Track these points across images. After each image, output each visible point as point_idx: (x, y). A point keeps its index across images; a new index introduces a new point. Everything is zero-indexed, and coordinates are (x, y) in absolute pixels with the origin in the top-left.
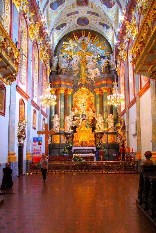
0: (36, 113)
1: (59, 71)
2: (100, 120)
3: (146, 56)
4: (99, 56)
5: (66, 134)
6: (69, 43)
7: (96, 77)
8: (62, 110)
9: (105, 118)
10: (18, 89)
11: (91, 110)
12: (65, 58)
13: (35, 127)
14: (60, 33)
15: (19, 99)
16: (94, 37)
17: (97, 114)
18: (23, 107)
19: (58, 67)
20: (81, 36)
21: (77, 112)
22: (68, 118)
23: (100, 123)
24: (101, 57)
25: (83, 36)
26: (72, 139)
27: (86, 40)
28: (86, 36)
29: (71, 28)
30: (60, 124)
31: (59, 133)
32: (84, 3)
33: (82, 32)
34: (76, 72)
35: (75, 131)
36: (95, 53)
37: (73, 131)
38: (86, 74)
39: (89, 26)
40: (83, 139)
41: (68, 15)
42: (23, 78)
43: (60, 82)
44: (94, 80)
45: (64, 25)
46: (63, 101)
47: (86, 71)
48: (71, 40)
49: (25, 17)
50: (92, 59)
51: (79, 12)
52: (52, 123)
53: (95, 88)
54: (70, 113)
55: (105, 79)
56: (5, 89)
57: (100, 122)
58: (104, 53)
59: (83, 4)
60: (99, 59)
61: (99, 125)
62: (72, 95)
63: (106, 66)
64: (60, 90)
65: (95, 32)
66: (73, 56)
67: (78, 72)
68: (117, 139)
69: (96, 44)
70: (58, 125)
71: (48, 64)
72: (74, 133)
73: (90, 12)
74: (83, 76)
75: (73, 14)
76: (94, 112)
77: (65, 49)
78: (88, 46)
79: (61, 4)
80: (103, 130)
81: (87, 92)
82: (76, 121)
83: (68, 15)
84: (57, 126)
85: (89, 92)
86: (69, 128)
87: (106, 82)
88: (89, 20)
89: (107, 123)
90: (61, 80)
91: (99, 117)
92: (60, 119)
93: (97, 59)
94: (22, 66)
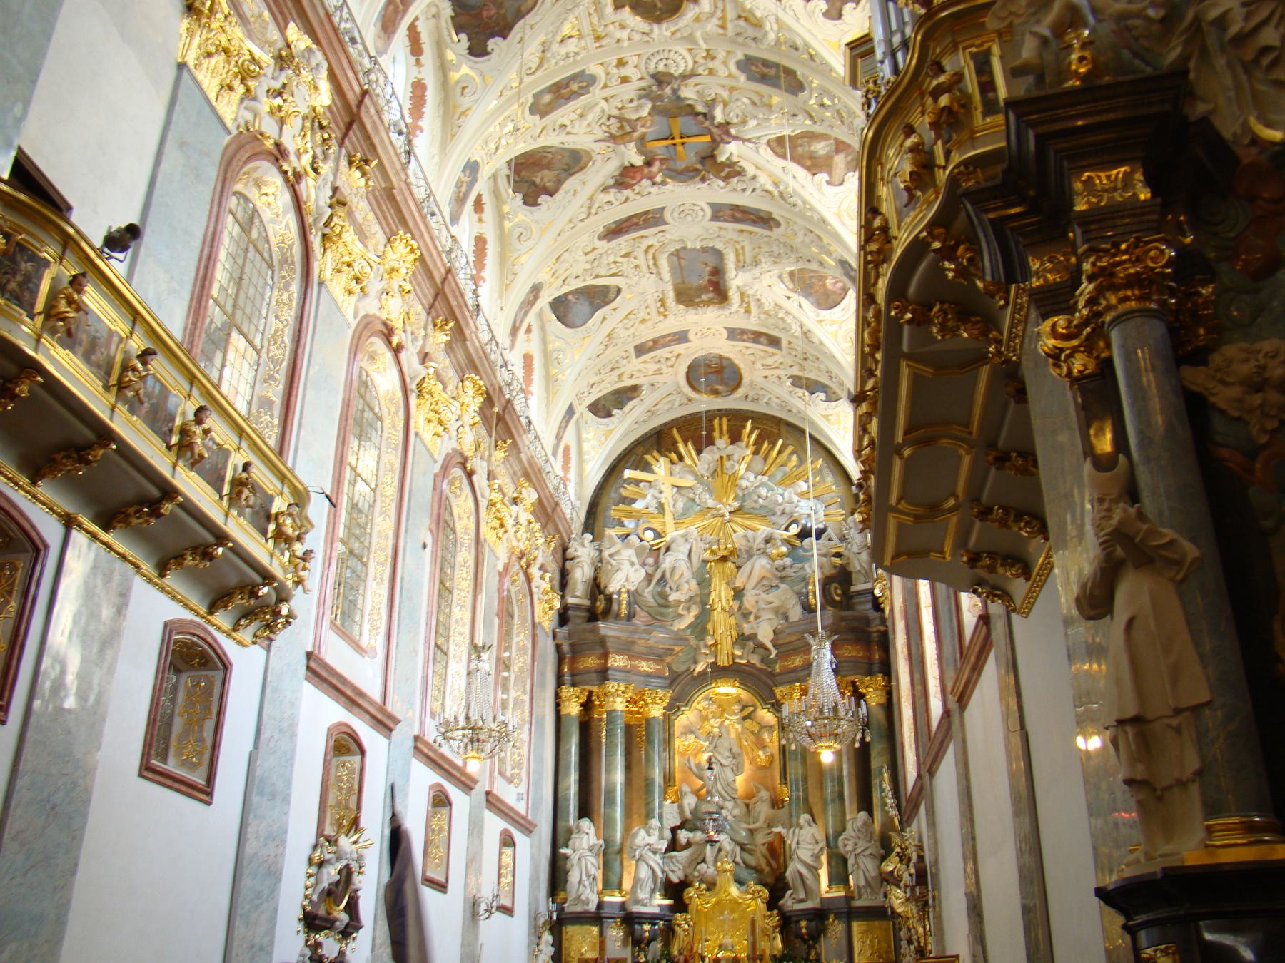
0: (451, 805)
1: (601, 605)
2: (805, 842)
3: (897, 464)
4: (794, 530)
5: (630, 920)
6: (653, 472)
7: (783, 632)
10: (319, 673)
11: (764, 794)
12: (628, 546)
13: (443, 880)
14: (611, 431)
15: (328, 725)
16: (774, 444)
17: (791, 816)
18: (357, 766)
19: (596, 587)
20: (711, 442)
21: (693, 807)
23: (809, 860)
24: (804, 534)
25: (722, 442)
27: (736, 457)
28: (735, 438)
29: (663, 406)
30: (606, 866)
31: (597, 918)
32: (711, 295)
33: (716, 422)
34: (688, 609)
35: (680, 906)
36: (775, 514)
37: (667, 902)
38: (738, 615)
39: (747, 397)
41: (640, 350)
42: (366, 627)
43: (605, 656)
44: (770, 646)
45: (629, 394)
47: (736, 605)
48: (662, 460)
49: (390, 343)
50: (762, 546)
51: (691, 336)
52: (560, 863)
54: (654, 810)
56: (226, 667)
57: (805, 854)
58: (821, 513)
59: (705, 297)
60: (797, 543)
61: (804, 871)
62: (668, 722)
63: (830, 571)
65: (778, 421)
66: (671, 533)
67: (695, 611)
68: (897, 939)
69: (779, 476)
71: (542, 568)
73: (743, 332)
74: (723, 629)
75: (664, 346)
76: (776, 803)
77: (634, 501)
78: (744, 483)
79: (606, 304)
81: (744, 707)
83: (640, 350)
84: (588, 876)
86: (648, 889)
88: (742, 366)
89: (845, 861)
90: (611, 649)
92: (605, 841)
93: (787, 542)
94: (365, 565)
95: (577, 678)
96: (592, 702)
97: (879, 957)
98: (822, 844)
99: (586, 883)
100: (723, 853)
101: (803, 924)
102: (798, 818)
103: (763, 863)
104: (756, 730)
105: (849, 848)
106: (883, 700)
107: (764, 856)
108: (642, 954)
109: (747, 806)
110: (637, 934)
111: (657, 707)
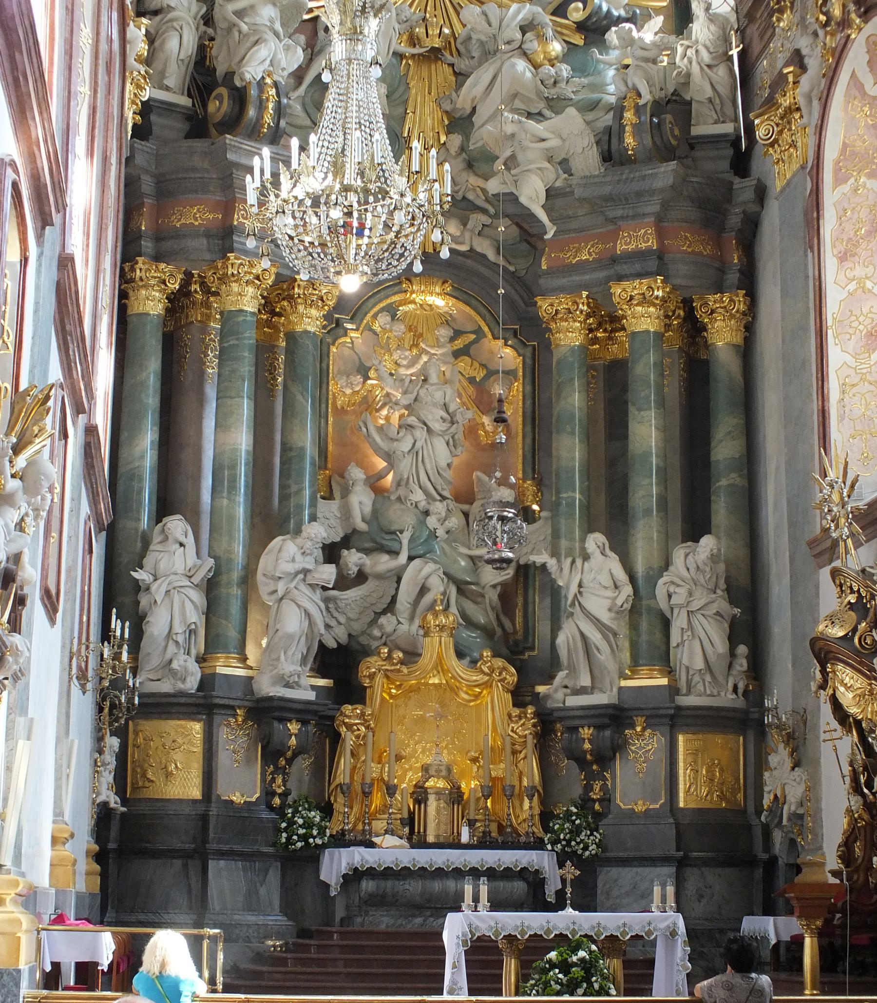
5: (264, 713)
8: (233, 481)
9: (640, 569)
21: (368, 509)
22: (289, 555)
23: (605, 617)
26: (324, 768)
37: (322, 682)
40: (425, 769)
47: (456, 140)
50: (519, 36)
53: (544, 294)
54: (300, 508)
55: (655, 208)
61: (595, 636)
64: (224, 279)
70: (195, 617)
72: (347, 709)
80: (624, 683)
81: (457, 334)
82: (352, 594)
85: (478, 332)
87: (661, 235)
89: (666, 624)
91: (586, 557)
92: (217, 559)
95: (168, 245)
96: (188, 294)
97: (722, 797)
98: (628, 590)
99: (180, 639)
101: (586, 732)
102: (583, 540)
103: (492, 616)
104: (480, 375)
106: (738, 339)
107: (492, 608)
108: (279, 781)
109: (466, 515)
111: (314, 312)
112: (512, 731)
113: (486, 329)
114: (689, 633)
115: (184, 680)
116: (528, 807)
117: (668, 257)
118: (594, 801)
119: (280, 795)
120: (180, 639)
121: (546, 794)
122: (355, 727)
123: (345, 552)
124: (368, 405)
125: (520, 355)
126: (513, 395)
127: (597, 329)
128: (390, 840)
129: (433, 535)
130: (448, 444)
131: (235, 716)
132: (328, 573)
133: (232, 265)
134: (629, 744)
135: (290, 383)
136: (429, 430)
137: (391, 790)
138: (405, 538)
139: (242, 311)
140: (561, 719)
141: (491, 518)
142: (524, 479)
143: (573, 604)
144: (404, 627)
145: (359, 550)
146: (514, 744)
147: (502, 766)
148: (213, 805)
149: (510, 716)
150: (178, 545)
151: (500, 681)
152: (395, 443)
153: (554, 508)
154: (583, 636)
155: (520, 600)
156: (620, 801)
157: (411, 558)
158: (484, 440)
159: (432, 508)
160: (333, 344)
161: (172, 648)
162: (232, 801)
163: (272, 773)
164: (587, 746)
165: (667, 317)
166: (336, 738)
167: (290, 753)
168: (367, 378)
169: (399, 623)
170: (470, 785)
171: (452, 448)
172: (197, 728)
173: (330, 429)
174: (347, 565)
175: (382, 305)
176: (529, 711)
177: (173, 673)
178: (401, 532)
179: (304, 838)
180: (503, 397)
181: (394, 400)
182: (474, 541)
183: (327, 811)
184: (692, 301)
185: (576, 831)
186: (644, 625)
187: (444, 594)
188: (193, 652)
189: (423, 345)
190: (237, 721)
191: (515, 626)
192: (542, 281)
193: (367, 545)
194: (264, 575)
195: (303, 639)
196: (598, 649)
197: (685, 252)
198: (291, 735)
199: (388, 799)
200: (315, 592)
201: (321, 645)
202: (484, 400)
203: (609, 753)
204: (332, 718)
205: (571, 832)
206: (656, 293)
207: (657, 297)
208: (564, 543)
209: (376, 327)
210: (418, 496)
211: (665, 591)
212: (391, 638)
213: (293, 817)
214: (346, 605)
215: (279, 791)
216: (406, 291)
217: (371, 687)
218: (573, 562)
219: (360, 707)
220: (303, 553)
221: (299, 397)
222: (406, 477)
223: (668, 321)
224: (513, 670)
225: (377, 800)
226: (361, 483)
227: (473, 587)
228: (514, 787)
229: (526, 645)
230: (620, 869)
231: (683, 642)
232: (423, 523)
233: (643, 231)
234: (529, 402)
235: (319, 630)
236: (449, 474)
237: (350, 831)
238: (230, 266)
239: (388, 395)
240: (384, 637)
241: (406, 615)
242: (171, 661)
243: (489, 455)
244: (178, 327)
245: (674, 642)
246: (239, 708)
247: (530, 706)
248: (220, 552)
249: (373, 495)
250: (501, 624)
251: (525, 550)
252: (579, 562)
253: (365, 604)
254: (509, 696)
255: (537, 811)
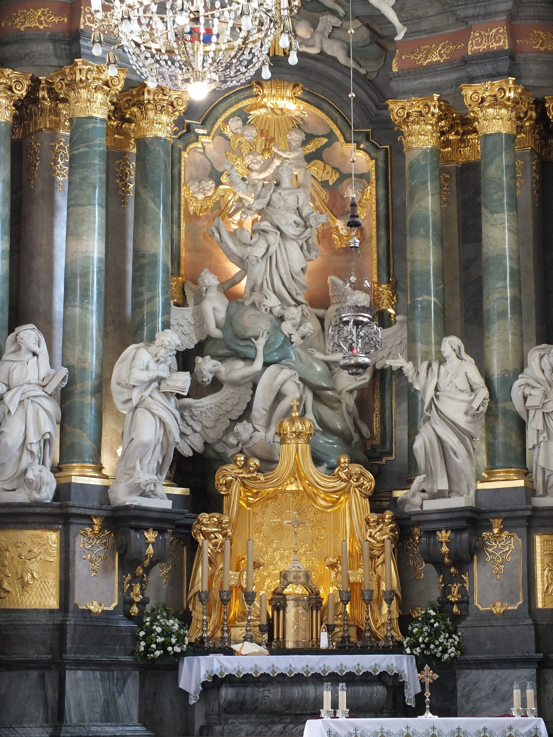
5: (121, 522)
8: (86, 289)
9: (496, 371)
21: (222, 315)
22: (144, 364)
23: (462, 420)
26: (182, 576)
30: (67, 418)
37: (178, 491)
40: (284, 576)
46: (98, 194)
53: (395, 97)
54: (153, 315)
61: (451, 440)
64: (72, 85)
70: (50, 427)
72: (204, 517)
80: (480, 486)
85: (330, 136)
87: (512, 34)
89: (521, 426)
91: (442, 361)
92: (70, 368)
98: (484, 393)
99: (35, 449)
100: (284, 405)
101: (444, 536)
102: (439, 343)
104: (332, 179)
105: (534, 400)
107: (349, 413)
108: (137, 589)
109: (321, 320)
110: (133, 547)
111: (164, 118)
112: (370, 536)
113: (338, 133)
114: (545, 435)
115: (39, 490)
116: (387, 611)
117: (520, 56)
118: (452, 603)
119: (138, 603)
120: (35, 449)
121: (405, 598)
122: (212, 535)
123: (199, 360)
124: (220, 211)
125: (372, 158)
126: (367, 201)
127: (449, 132)
128: (249, 647)
129: (288, 340)
130: (301, 248)
131: (91, 525)
132: (182, 381)
133: (80, 70)
134: (487, 546)
135: (141, 190)
136: (282, 235)
137: (250, 597)
138: (260, 344)
139: (91, 118)
140: (418, 523)
141: (347, 323)
142: (379, 283)
143: (429, 409)
144: (260, 435)
145: (213, 357)
146: (372, 550)
147: (361, 571)
148: (70, 614)
149: (368, 522)
150: (31, 355)
151: (357, 487)
152: (249, 248)
153: (410, 312)
154: (440, 440)
155: (377, 404)
156: (479, 604)
157: (266, 365)
158: (338, 244)
159: (286, 314)
160: (185, 150)
161: (26, 458)
162: (90, 611)
163: (130, 582)
164: (445, 549)
165: (519, 118)
166: (194, 546)
167: (147, 562)
168: (219, 183)
169: (255, 430)
170: (328, 592)
171: (307, 253)
172: (53, 538)
173: (183, 236)
174: (202, 372)
175: (233, 110)
176: (387, 516)
177: (29, 483)
178: (256, 338)
179: (163, 646)
180: (357, 201)
181: (247, 204)
182: (330, 346)
183: (186, 619)
184: (544, 102)
185: (435, 634)
186: (500, 428)
187: (300, 400)
188: (48, 462)
189: (274, 150)
190: (93, 530)
191: (373, 433)
192: (393, 84)
193: (222, 352)
194: (118, 384)
195: (159, 447)
196: (455, 453)
197: (537, 51)
198: (148, 544)
199: (247, 606)
200: (169, 399)
201: (177, 453)
202: (337, 204)
203: (466, 556)
204: (189, 527)
205: (430, 635)
206: (508, 94)
207: (509, 99)
208: (420, 347)
209: (228, 132)
210: (273, 301)
211: (520, 393)
212: (248, 445)
213: (152, 625)
214: (201, 413)
215: (137, 599)
216: (257, 96)
217: (227, 495)
218: (430, 365)
219: (217, 515)
220: (157, 361)
221: (151, 204)
222: (260, 282)
223: (519, 123)
224: (370, 476)
225: (235, 607)
226: (215, 289)
227: (330, 393)
228: (372, 591)
229: (384, 451)
230: (480, 671)
231: (539, 443)
232: (278, 329)
233: (494, 31)
234: (382, 206)
235: (174, 439)
236: (303, 279)
237: (209, 638)
238: (78, 72)
239: (240, 200)
240: (240, 445)
241: (262, 421)
242: (25, 471)
243: (343, 260)
244: (27, 135)
245: (529, 445)
246: (96, 517)
247: (388, 511)
248: (73, 361)
249: (226, 301)
250: (358, 430)
251: (380, 355)
252: (435, 366)
253: (221, 412)
254: (367, 501)
255: (395, 615)
